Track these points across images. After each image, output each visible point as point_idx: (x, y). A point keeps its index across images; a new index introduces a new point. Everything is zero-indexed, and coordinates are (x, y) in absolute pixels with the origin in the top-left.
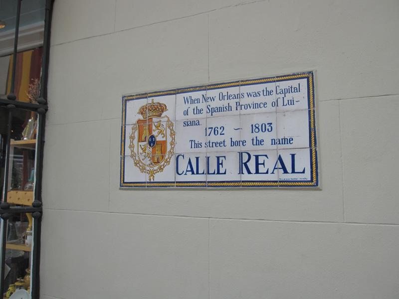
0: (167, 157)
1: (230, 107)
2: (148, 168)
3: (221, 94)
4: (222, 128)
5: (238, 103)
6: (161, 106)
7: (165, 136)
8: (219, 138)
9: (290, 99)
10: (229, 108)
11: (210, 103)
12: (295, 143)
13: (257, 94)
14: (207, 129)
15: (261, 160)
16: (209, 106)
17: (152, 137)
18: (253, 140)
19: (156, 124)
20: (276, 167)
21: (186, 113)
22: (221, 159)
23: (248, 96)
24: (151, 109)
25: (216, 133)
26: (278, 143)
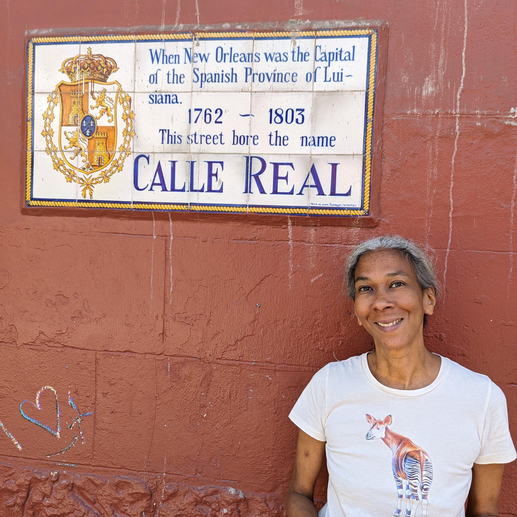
0: (117, 156)
1: (234, 76)
2: (80, 175)
3: (220, 50)
4: (219, 111)
5: (249, 70)
6: (106, 63)
8: (212, 129)
10: (232, 77)
12: (339, 147)
13: (283, 57)
14: (193, 111)
15: (282, 171)
16: (196, 71)
17: (89, 119)
18: (270, 135)
20: (306, 184)
21: (153, 79)
22: (215, 166)
23: (267, 59)
25: (208, 120)
26: (312, 143)
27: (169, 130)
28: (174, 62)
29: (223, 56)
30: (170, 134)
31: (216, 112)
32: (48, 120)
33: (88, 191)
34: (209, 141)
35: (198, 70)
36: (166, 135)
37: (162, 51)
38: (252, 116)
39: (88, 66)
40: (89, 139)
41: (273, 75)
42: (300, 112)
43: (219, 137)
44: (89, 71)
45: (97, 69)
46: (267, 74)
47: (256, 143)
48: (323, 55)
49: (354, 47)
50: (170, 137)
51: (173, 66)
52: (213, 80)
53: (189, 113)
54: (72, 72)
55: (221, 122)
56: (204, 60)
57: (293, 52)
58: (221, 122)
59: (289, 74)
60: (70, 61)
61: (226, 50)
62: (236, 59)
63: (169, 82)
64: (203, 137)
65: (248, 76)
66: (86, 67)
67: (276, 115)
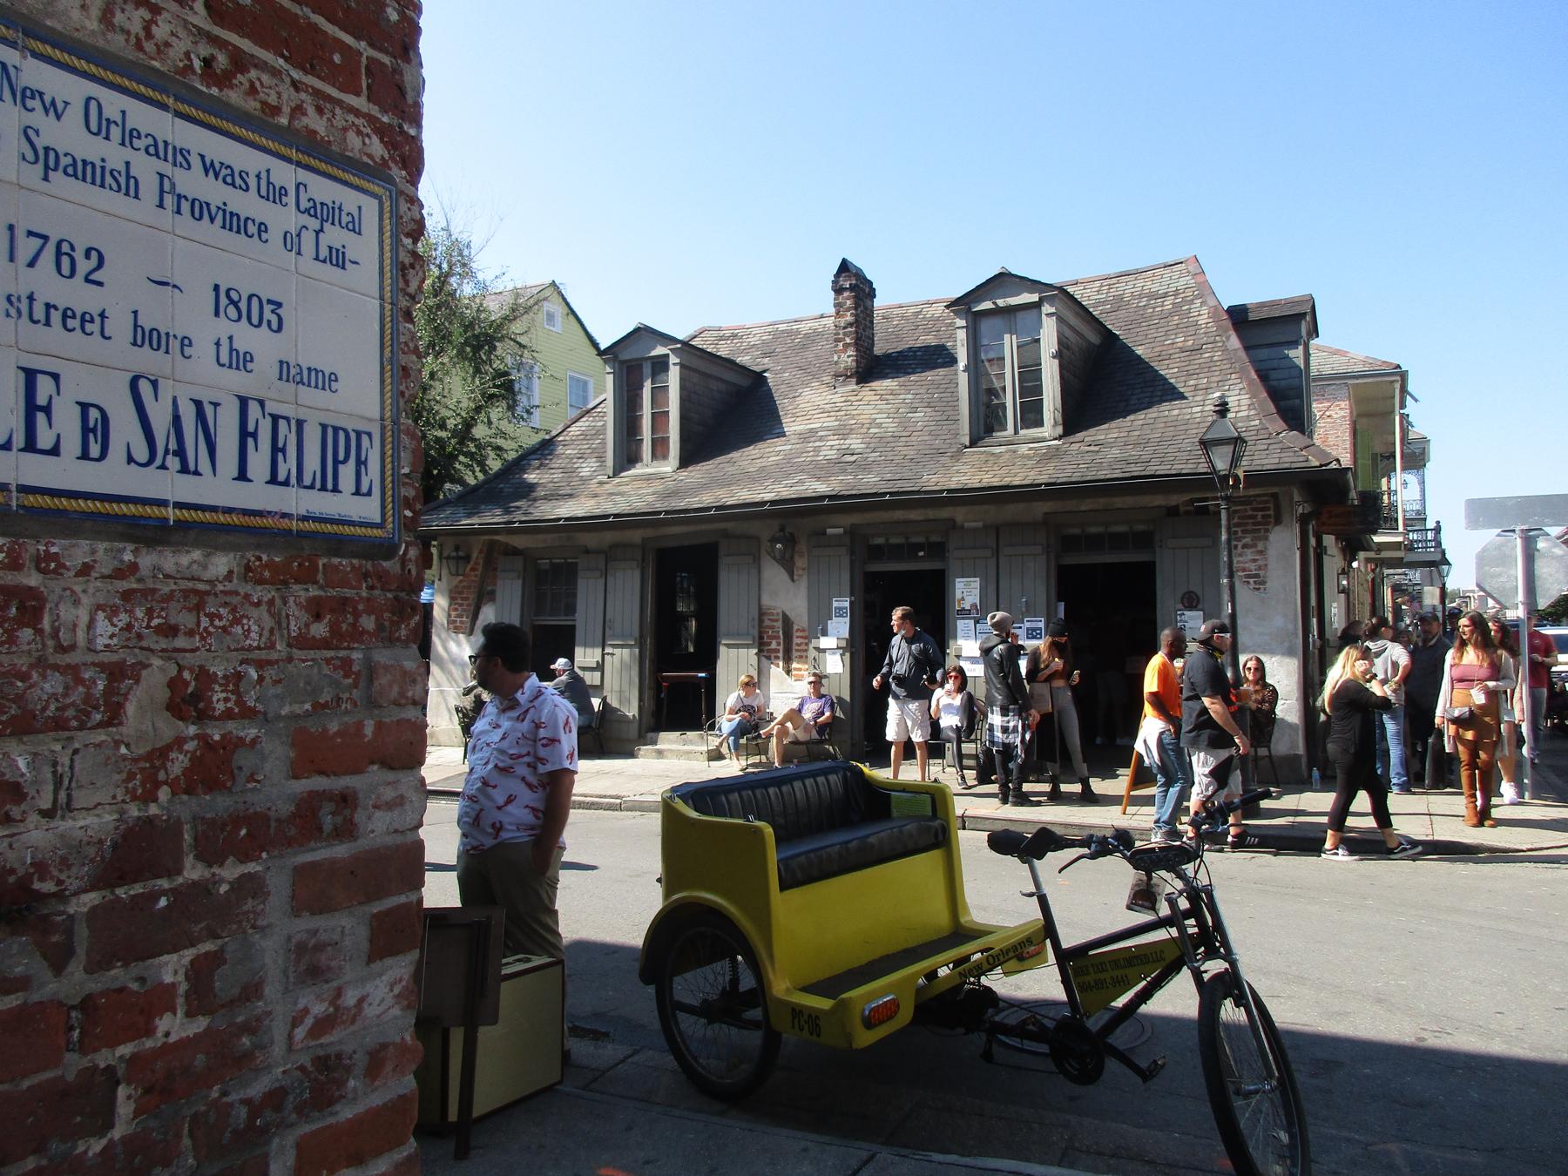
4: (94, 254)
10: (128, 185)
11: (38, 118)
14: (20, 234)
18: (218, 344)
23: (207, 175)
25: (66, 270)
29: (104, 123)
31: (88, 256)
38: (176, 291)
41: (221, 213)
42: (273, 307)
43: (98, 320)
47: (186, 354)
48: (311, 204)
49: (360, 208)
55: (100, 284)
57: (258, 176)
58: (100, 284)
59: (253, 221)
61: (111, 112)
62: (136, 142)
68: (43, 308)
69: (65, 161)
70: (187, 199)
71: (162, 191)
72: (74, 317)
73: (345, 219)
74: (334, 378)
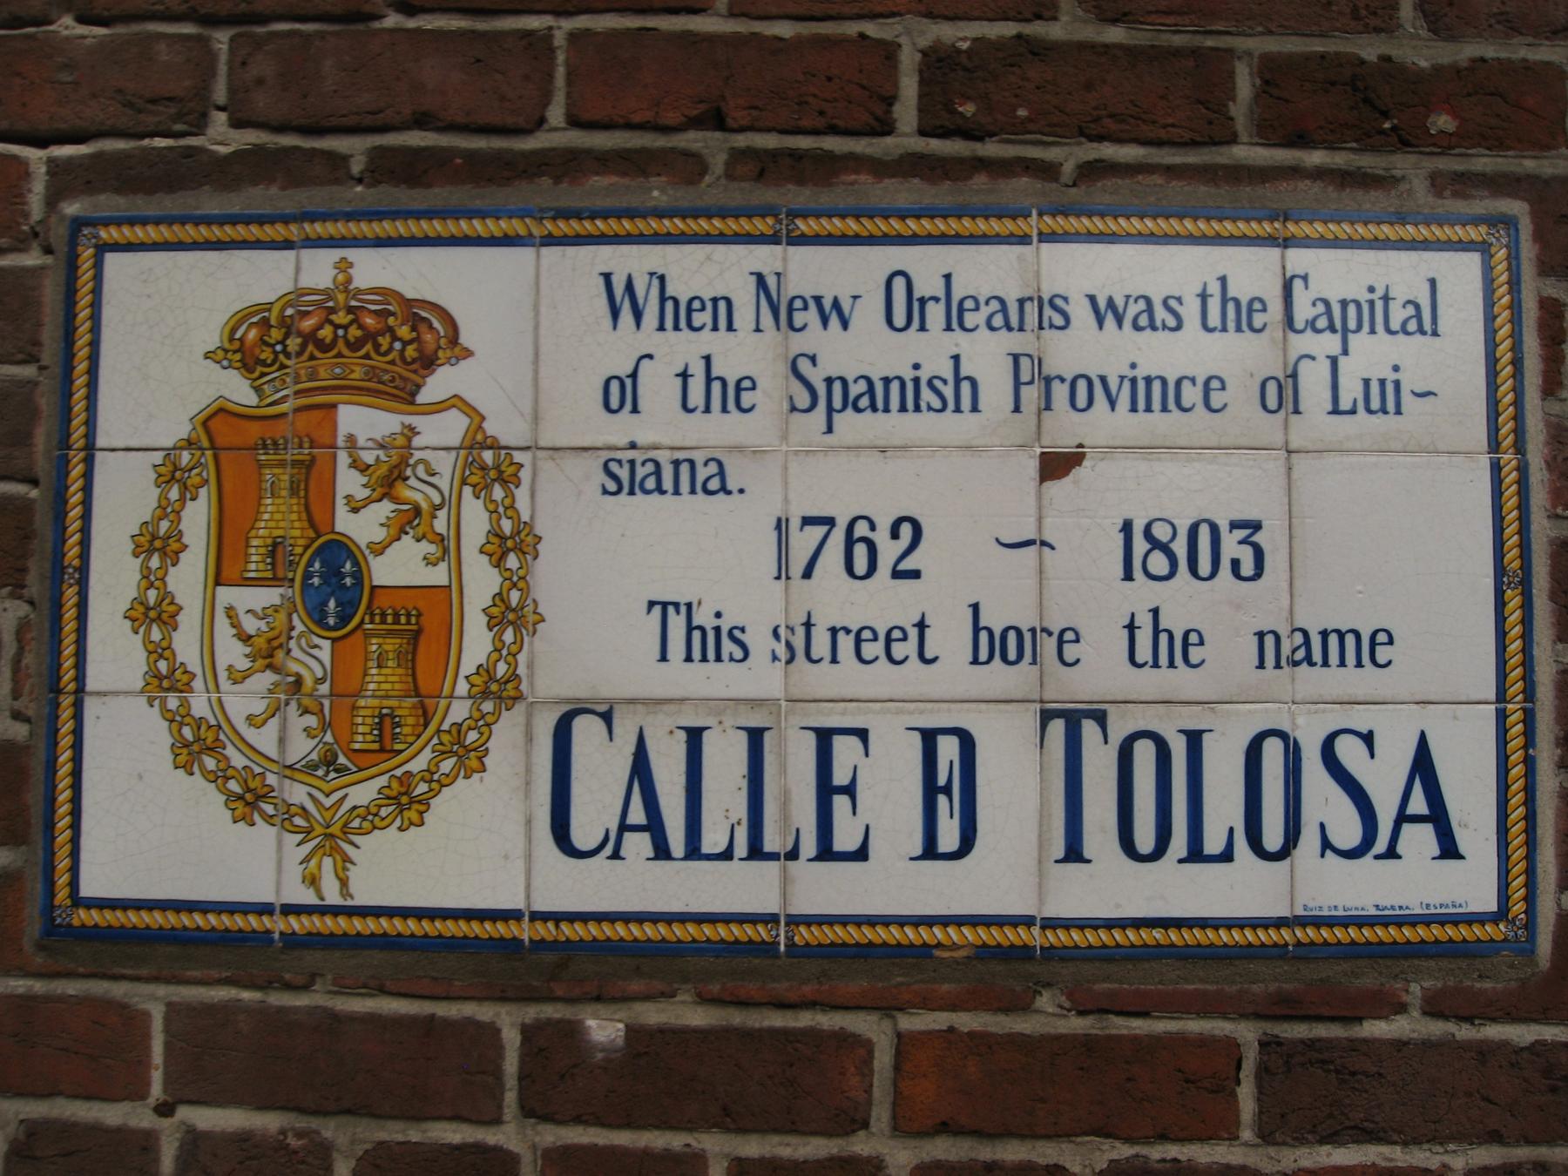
0: (459, 711)
1: (966, 387)
2: (297, 794)
3: (899, 285)
4: (906, 530)
7: (446, 548)
9: (1375, 375)
11: (811, 335)
13: (1161, 314)
14: (795, 523)
18: (1131, 627)
19: (368, 457)
23: (1101, 326)
24: (326, 333)
25: (861, 565)
27: (689, 606)
28: (710, 325)
29: (916, 305)
30: (696, 622)
31: (895, 535)
32: (155, 562)
33: (328, 863)
34: (869, 650)
35: (813, 359)
36: (677, 623)
37: (656, 282)
38: (1046, 550)
39: (336, 336)
40: (334, 640)
41: (1127, 385)
42: (1242, 533)
43: (913, 633)
44: (340, 355)
45: (377, 346)
46: (1103, 380)
47: (1069, 658)
48: (1321, 308)
49: (1433, 283)
50: (697, 635)
51: (707, 341)
52: (880, 404)
53: (775, 535)
54: (264, 363)
55: (915, 574)
56: (834, 321)
57: (1204, 297)
58: (915, 574)
59: (1193, 380)
60: (254, 320)
61: (928, 285)
62: (970, 319)
63: (691, 405)
64: (841, 636)
65: (1024, 390)
66: (328, 341)
67: (1148, 546)
68: (828, 636)
69: (856, 389)
70: (1063, 380)
71: (1017, 384)
72: (875, 639)
73: (1398, 315)
74: (1382, 637)
